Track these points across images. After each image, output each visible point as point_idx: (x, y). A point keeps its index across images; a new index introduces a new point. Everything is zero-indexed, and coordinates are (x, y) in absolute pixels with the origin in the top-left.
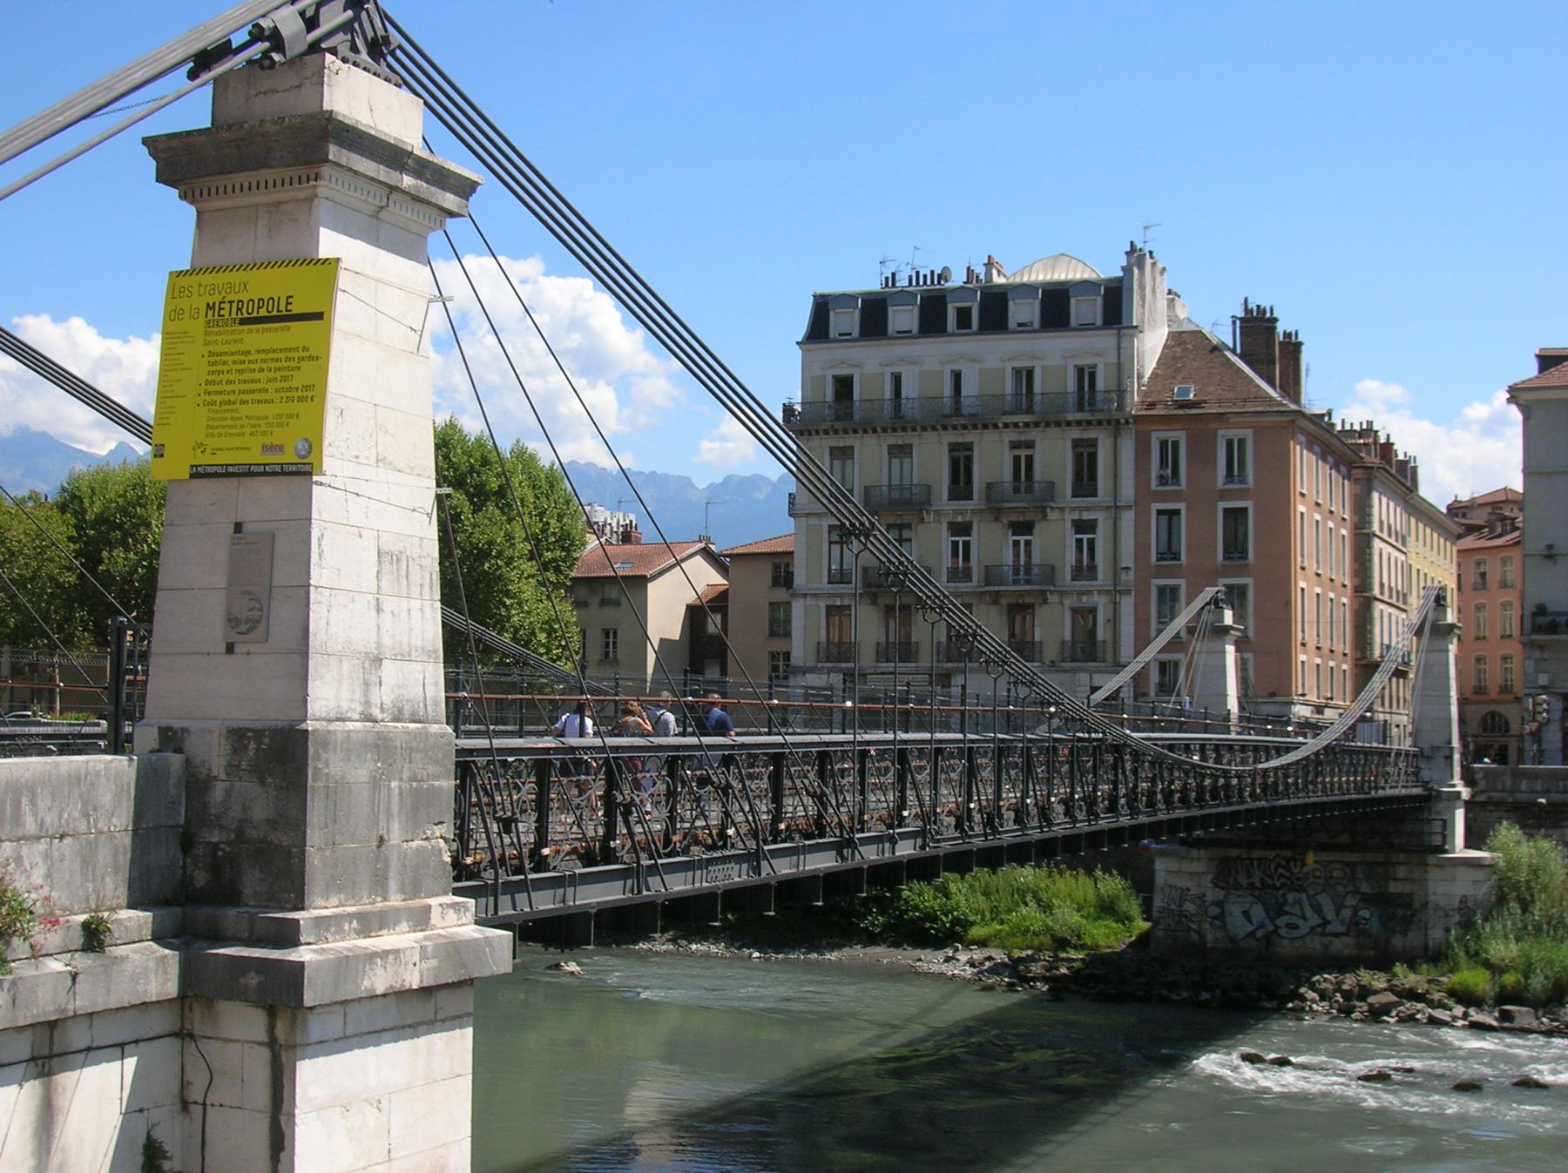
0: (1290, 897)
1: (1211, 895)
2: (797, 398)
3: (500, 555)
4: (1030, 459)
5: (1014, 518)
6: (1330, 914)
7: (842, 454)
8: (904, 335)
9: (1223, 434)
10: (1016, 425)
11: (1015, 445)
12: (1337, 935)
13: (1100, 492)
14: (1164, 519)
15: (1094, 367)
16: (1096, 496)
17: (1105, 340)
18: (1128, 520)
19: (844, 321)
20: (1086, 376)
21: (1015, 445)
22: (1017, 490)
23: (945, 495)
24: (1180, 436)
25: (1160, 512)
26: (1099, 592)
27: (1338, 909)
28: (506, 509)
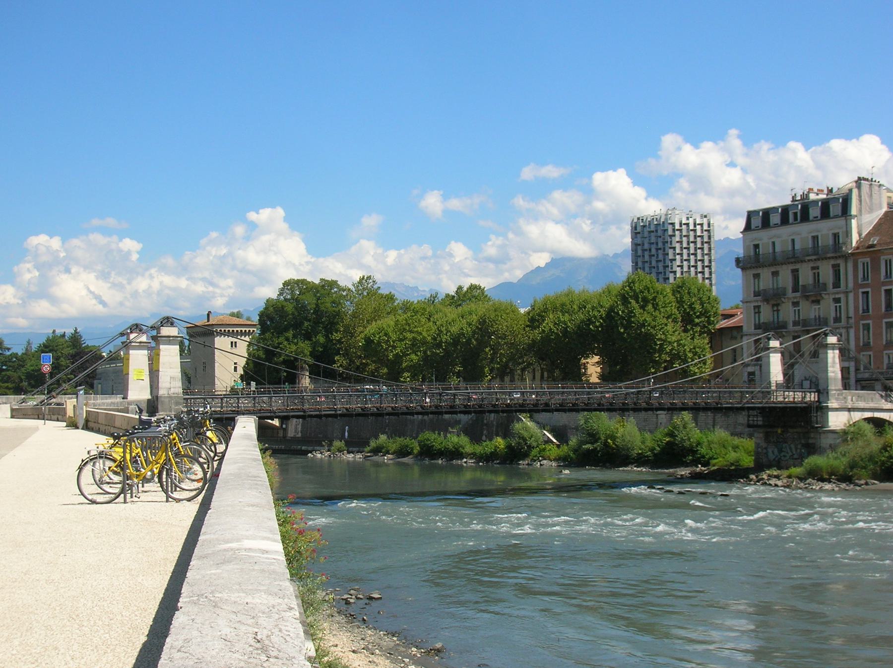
0: (784, 445)
1: (764, 445)
2: (742, 256)
3: (649, 325)
4: (818, 273)
5: (813, 298)
6: (794, 450)
7: (757, 276)
8: (776, 225)
9: (883, 258)
10: (811, 260)
11: (813, 268)
12: (796, 459)
13: (842, 286)
14: (865, 295)
15: (838, 233)
16: (840, 287)
17: (841, 222)
18: (851, 296)
19: (757, 222)
20: (836, 236)
21: (813, 268)
22: (815, 287)
23: (791, 291)
24: (868, 260)
25: (863, 293)
26: (843, 328)
27: (796, 449)
28: (655, 307)
